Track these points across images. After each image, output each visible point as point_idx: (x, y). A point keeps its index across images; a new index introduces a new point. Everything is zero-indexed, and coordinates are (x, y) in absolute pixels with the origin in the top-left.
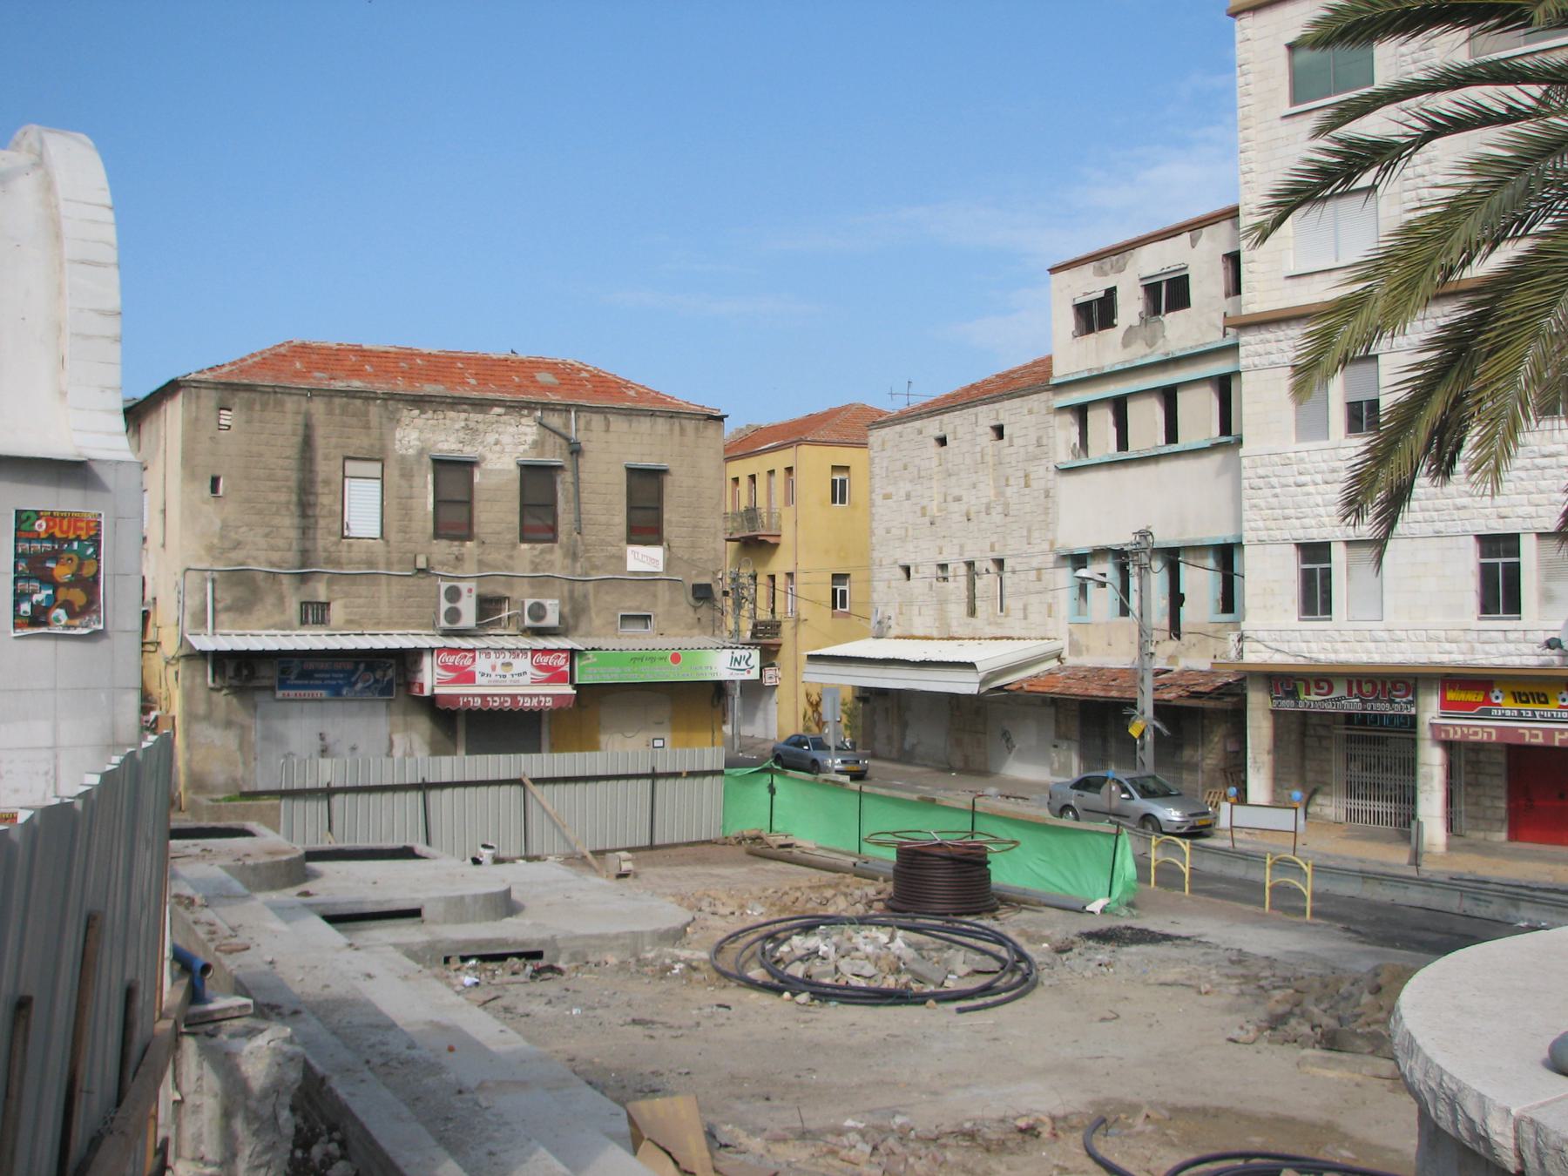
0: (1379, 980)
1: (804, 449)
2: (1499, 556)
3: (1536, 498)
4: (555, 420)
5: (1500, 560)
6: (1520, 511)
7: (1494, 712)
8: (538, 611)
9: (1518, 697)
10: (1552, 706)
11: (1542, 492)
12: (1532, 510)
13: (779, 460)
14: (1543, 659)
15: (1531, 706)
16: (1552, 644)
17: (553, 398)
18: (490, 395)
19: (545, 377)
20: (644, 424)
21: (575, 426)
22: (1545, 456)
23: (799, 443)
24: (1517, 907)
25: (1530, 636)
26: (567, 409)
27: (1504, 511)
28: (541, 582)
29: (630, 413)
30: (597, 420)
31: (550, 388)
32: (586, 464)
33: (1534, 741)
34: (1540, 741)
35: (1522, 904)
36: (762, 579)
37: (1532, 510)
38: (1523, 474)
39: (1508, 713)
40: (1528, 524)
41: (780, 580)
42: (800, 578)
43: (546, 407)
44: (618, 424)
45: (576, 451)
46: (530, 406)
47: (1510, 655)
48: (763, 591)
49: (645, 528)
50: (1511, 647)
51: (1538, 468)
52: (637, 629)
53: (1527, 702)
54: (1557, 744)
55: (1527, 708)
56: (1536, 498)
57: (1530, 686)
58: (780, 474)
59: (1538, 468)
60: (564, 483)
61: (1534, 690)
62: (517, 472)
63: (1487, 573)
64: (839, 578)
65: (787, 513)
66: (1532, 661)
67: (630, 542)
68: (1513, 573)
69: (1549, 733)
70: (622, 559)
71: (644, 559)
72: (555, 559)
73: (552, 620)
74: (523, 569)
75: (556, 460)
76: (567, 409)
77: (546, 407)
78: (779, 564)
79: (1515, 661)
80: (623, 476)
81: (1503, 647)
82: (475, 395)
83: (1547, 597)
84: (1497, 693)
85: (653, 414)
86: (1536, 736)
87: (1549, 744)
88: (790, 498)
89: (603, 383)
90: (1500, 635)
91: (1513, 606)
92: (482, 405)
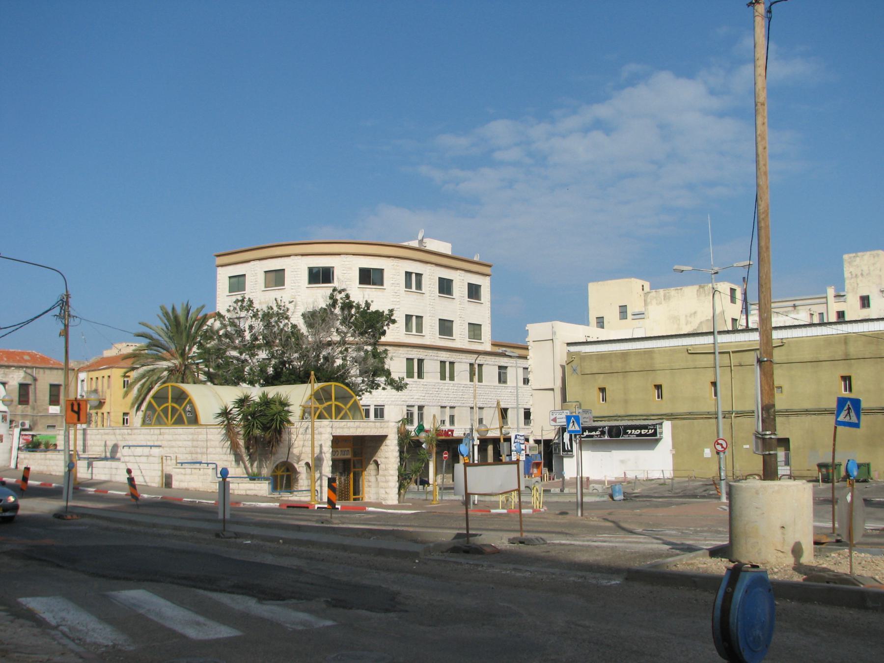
1: (114, 370)
4: (29, 371)
8: (23, 424)
13: (106, 373)
17: (29, 364)
18: (11, 364)
19: (26, 357)
20: (55, 372)
21: (35, 372)
23: (112, 367)
26: (33, 368)
28: (24, 416)
29: (51, 369)
30: (41, 371)
31: (27, 361)
32: (38, 383)
36: (100, 414)
41: (105, 414)
42: (112, 414)
43: (27, 367)
44: (47, 372)
45: (35, 380)
46: (22, 367)
48: (99, 419)
49: (54, 401)
52: (51, 429)
58: (106, 377)
60: (31, 389)
62: (18, 386)
64: (125, 414)
65: (108, 392)
67: (50, 404)
70: (48, 410)
71: (54, 410)
72: (28, 409)
73: (27, 426)
74: (19, 412)
75: (29, 382)
76: (33, 368)
77: (27, 367)
78: (105, 409)
80: (48, 387)
82: (6, 364)
85: (57, 369)
88: (109, 387)
89: (44, 360)
92: (8, 367)
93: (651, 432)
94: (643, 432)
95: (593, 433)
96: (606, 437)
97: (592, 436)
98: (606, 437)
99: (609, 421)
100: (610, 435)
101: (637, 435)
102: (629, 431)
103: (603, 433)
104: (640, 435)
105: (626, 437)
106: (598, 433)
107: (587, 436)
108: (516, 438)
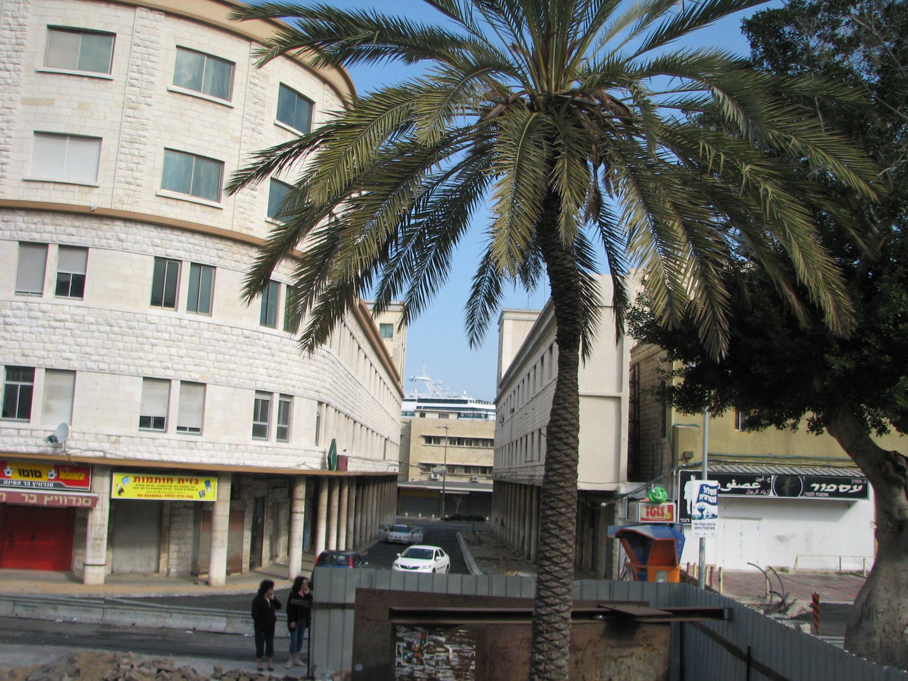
0: (77, 665)
2: (18, 380)
3: (48, 346)
5: (20, 384)
6: (38, 353)
7: (6, 482)
9: (22, 473)
10: (44, 479)
11: (52, 343)
12: (45, 353)
14: (42, 449)
15: (31, 479)
16: (52, 439)
22: (57, 321)
24: (56, 609)
25: (35, 433)
27: (27, 352)
33: (31, 501)
34: (35, 501)
35: (60, 607)
37: (45, 353)
38: (42, 330)
39: (15, 483)
40: (41, 362)
47: (19, 444)
50: (22, 440)
51: (52, 327)
53: (28, 476)
54: (45, 503)
55: (27, 480)
56: (48, 346)
57: (30, 466)
59: (52, 327)
61: (33, 468)
63: (10, 391)
66: (34, 450)
68: (28, 393)
69: (41, 497)
79: (23, 449)
81: (16, 440)
83: (47, 409)
84: (8, 469)
86: (33, 498)
87: (41, 503)
90: (15, 432)
91: (25, 413)
93: (856, 489)
94: (842, 488)
95: (747, 486)
96: (771, 495)
97: (744, 491)
98: (771, 495)
99: (755, 464)
100: (779, 491)
101: (831, 494)
102: (816, 486)
103: (765, 486)
104: (837, 493)
105: (809, 496)
106: (755, 486)
107: (734, 491)
108: (701, 491)
